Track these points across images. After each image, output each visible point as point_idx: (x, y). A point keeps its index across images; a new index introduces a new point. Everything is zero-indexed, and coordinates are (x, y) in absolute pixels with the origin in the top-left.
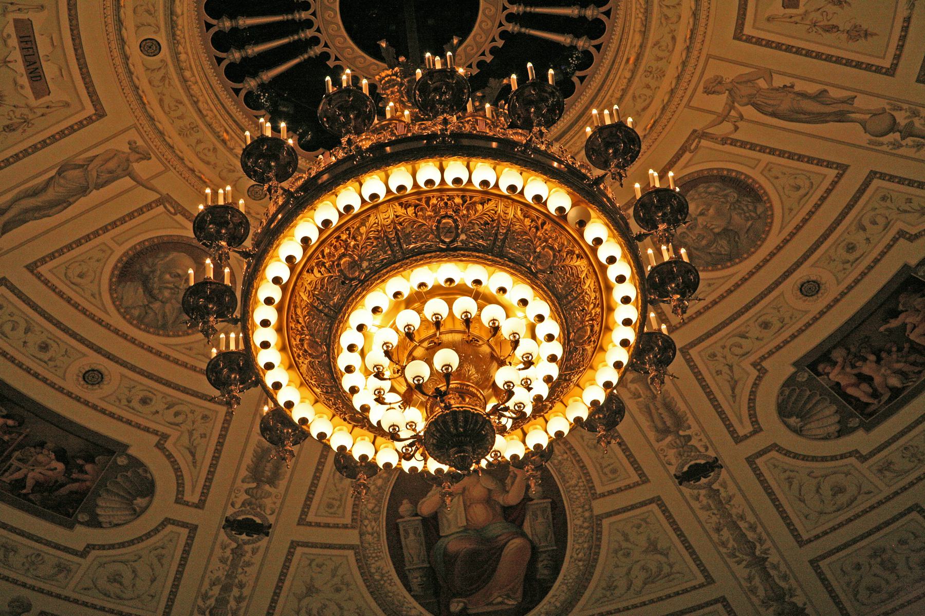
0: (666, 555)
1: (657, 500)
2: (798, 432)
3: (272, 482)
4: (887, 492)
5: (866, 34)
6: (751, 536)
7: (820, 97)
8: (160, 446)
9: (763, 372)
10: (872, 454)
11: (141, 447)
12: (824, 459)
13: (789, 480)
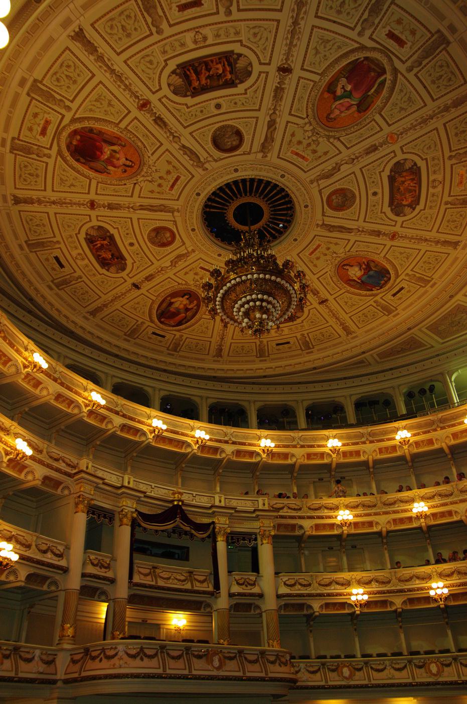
0: (316, 47)
1: (302, 69)
2: (250, 64)
3: (375, 145)
4: (242, 23)
5: (167, 161)
6: (289, 36)
7: (185, 153)
8: (383, 171)
9: (246, 90)
10: (237, 41)
11: (387, 172)
12: (250, 49)
13: (265, 49)
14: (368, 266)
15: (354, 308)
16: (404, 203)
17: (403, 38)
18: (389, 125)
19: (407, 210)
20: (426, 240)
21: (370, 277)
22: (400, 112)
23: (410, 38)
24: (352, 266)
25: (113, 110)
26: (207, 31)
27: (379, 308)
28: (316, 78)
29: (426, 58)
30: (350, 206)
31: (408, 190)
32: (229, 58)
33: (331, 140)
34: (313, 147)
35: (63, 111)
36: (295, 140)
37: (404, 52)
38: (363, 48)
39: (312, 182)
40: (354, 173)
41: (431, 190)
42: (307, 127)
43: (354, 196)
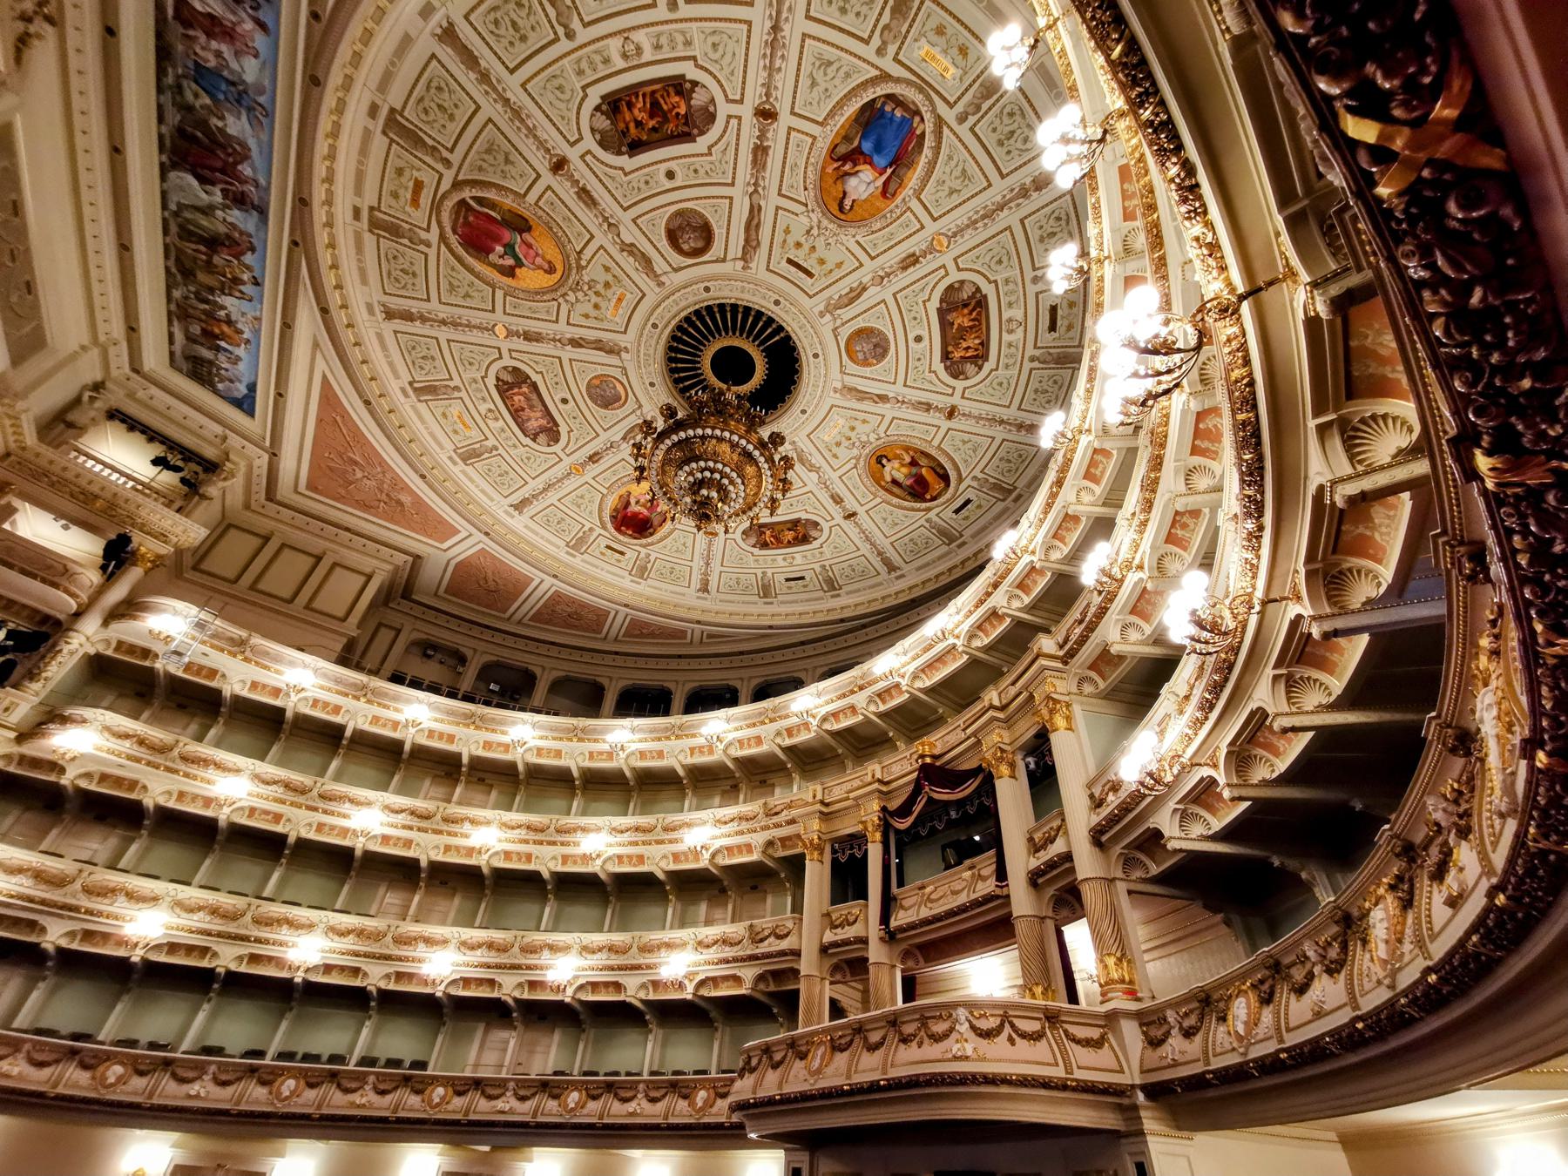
2: (505, 368)
8: (622, 169)
11: (624, 161)
14: (846, 157)
15: (972, 169)
16: (682, 110)
17: (411, 184)
18: (539, 176)
19: (699, 99)
20: (776, 28)
21: (878, 148)
22: (512, 163)
23: (407, 173)
24: (845, 193)
25: (587, 496)
26: (483, 408)
27: (985, 107)
28: (499, 294)
29: (425, 143)
30: (702, 216)
31: (655, 109)
32: (504, 388)
33: (583, 263)
34: (599, 287)
35: (595, 534)
36: (593, 313)
37: (428, 178)
38: (443, 238)
39: (661, 284)
40: (634, 221)
41: (648, 56)
42: (571, 297)
43: (679, 213)
